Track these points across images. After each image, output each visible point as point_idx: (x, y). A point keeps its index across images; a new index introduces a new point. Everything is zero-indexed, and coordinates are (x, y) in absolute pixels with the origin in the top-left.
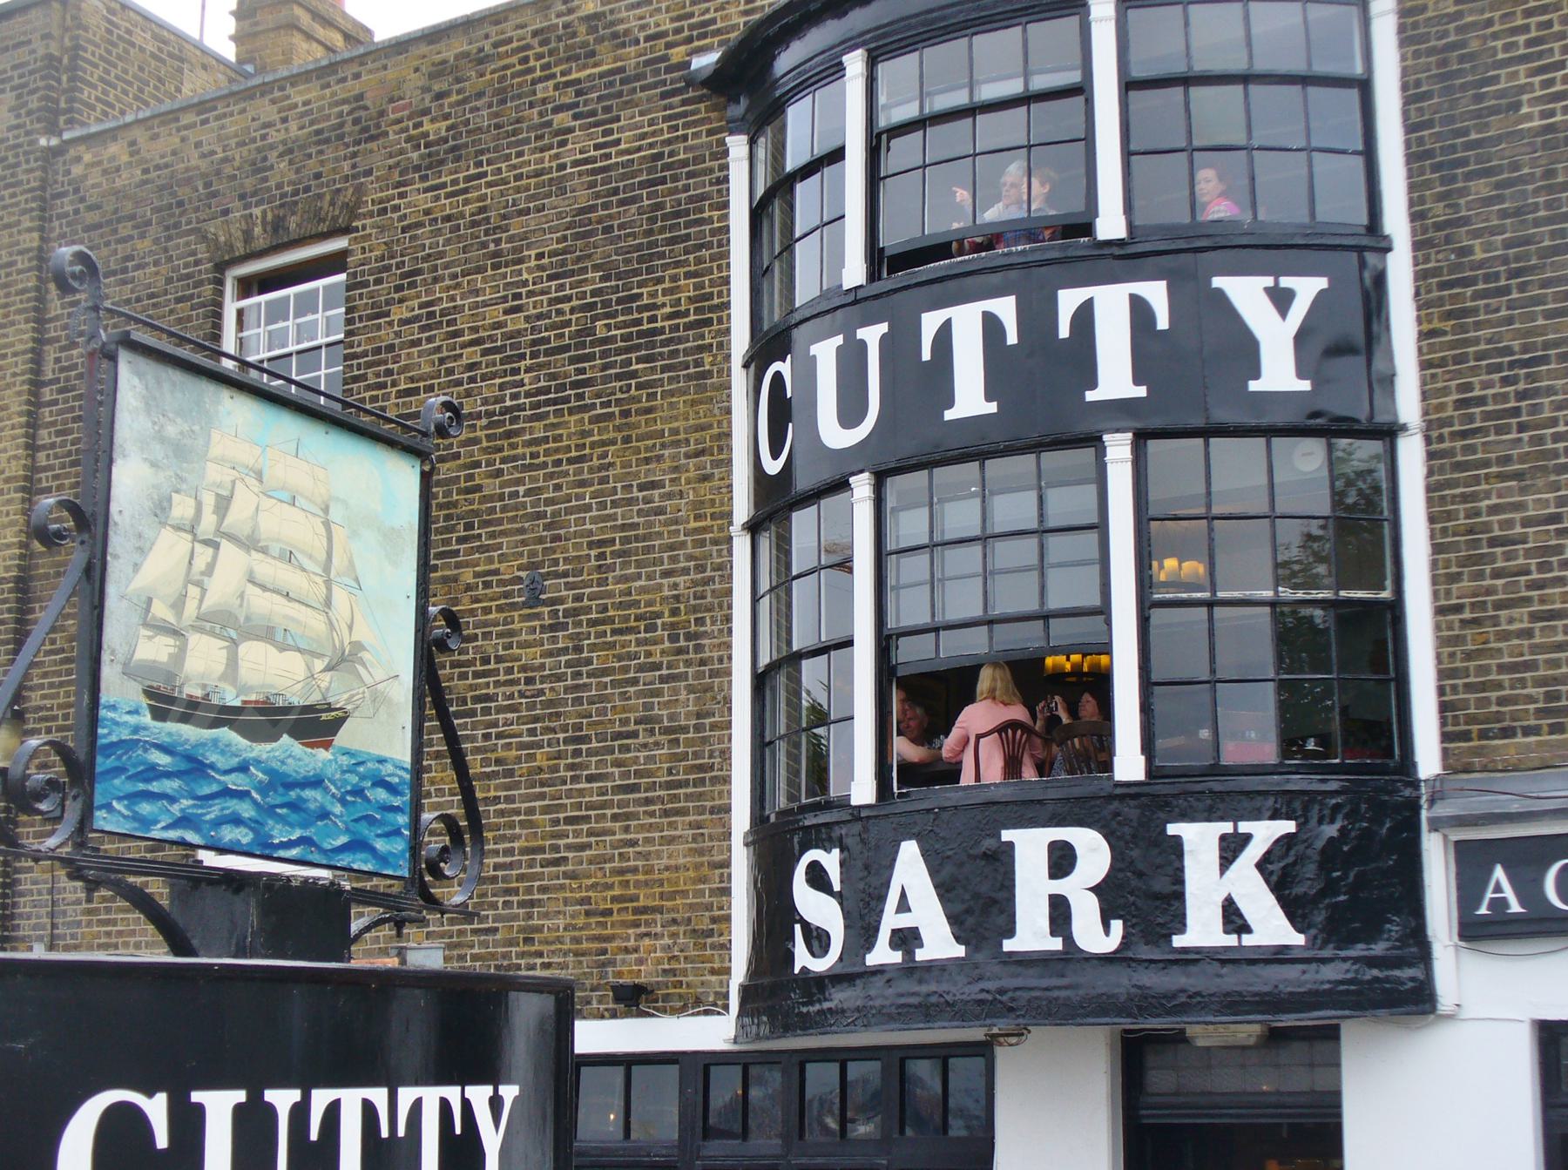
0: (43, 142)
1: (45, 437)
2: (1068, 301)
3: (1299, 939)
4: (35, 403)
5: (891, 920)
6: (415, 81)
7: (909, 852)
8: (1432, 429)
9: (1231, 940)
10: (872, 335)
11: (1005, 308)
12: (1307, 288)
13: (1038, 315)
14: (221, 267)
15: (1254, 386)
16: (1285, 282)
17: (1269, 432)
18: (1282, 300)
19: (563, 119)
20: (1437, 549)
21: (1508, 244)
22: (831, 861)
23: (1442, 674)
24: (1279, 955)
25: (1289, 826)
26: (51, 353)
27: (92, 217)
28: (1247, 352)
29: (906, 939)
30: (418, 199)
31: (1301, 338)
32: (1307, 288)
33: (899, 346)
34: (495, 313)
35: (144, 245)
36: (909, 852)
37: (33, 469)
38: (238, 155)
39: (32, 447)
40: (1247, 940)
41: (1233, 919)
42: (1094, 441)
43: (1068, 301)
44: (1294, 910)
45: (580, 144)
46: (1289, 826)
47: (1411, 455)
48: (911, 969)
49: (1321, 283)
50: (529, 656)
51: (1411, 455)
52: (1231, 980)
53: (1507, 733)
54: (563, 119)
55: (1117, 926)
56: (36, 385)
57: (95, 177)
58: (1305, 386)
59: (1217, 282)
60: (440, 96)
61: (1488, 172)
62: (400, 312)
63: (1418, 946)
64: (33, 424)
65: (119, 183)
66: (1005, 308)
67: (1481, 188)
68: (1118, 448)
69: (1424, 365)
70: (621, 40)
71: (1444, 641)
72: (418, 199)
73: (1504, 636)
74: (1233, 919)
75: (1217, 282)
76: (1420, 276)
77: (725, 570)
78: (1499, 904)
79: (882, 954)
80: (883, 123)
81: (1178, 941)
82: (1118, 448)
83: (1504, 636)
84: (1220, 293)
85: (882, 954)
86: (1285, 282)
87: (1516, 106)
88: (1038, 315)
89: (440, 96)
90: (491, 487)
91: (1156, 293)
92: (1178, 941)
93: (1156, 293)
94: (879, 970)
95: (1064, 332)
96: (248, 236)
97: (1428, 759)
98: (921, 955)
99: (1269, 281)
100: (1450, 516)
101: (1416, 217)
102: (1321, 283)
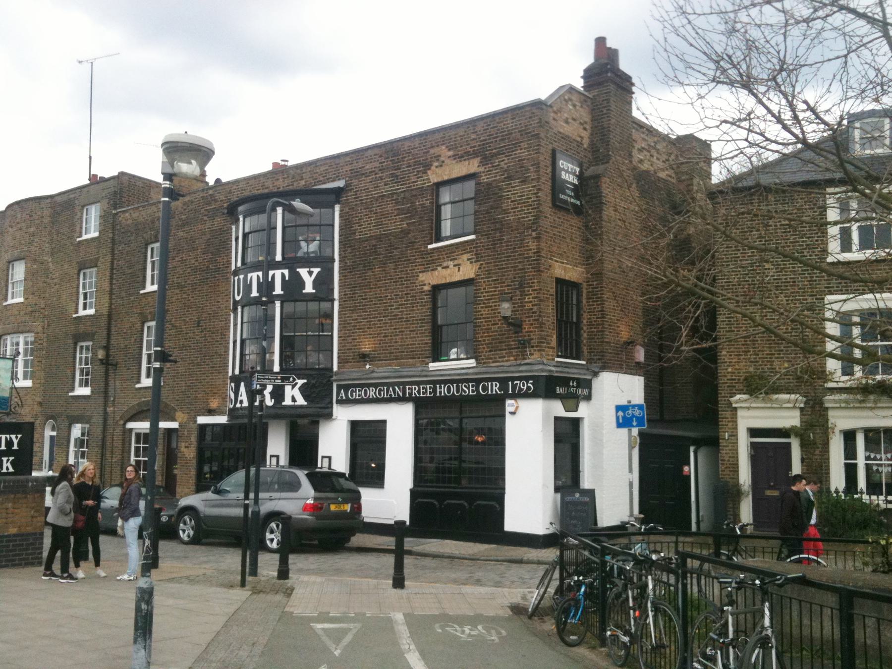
0: (113, 212)
1: (114, 282)
2: (271, 273)
3: (306, 403)
4: (112, 274)
5: (240, 398)
6: (180, 205)
7: (242, 384)
8: (340, 299)
9: (293, 404)
10: (242, 277)
11: (260, 274)
12: (316, 271)
13: (266, 275)
14: (147, 245)
15: (304, 291)
16: (312, 269)
17: (307, 301)
18: (310, 273)
19: (205, 218)
20: (339, 324)
21: (353, 262)
22: (233, 385)
23: (339, 350)
24: (301, 407)
25: (305, 381)
26: (115, 262)
27: (123, 230)
28: (302, 284)
29: (241, 402)
30: (181, 234)
31: (314, 282)
32: (316, 271)
33: (245, 279)
34: (193, 261)
35: (132, 238)
36: (242, 384)
37: (111, 290)
38: (150, 219)
39: (111, 284)
40: (296, 404)
41: (294, 399)
42: (273, 302)
43: (271, 273)
44: (305, 397)
45: (208, 225)
46: (305, 381)
47: (336, 305)
48: (242, 408)
49: (319, 269)
50: (197, 338)
51: (336, 305)
52: (293, 412)
53: (347, 362)
54: (205, 218)
55: (273, 400)
56: (112, 269)
57: (124, 221)
58: (314, 291)
59: (298, 270)
60: (185, 210)
61: (350, 247)
62: (177, 259)
63: (331, 403)
64: (111, 278)
65: (128, 222)
66: (260, 274)
67: (349, 250)
68: (278, 304)
69: (340, 286)
70: (216, 201)
71: (339, 343)
72: (181, 234)
73: (348, 343)
74: (294, 399)
75: (298, 270)
76: (340, 267)
77: (230, 320)
78: (342, 397)
79: (238, 405)
80: (247, 230)
81: (283, 404)
82: (278, 304)
83: (348, 343)
84: (298, 272)
85: (238, 405)
86: (312, 269)
87: (355, 233)
88: (266, 275)
89: (185, 210)
90: (192, 300)
91: (286, 272)
92: (283, 404)
93: (286, 272)
94: (238, 408)
95: (270, 280)
96: (151, 239)
97: (335, 368)
98: (243, 405)
99: (308, 269)
100: (342, 318)
101: (340, 255)
102: (319, 269)
